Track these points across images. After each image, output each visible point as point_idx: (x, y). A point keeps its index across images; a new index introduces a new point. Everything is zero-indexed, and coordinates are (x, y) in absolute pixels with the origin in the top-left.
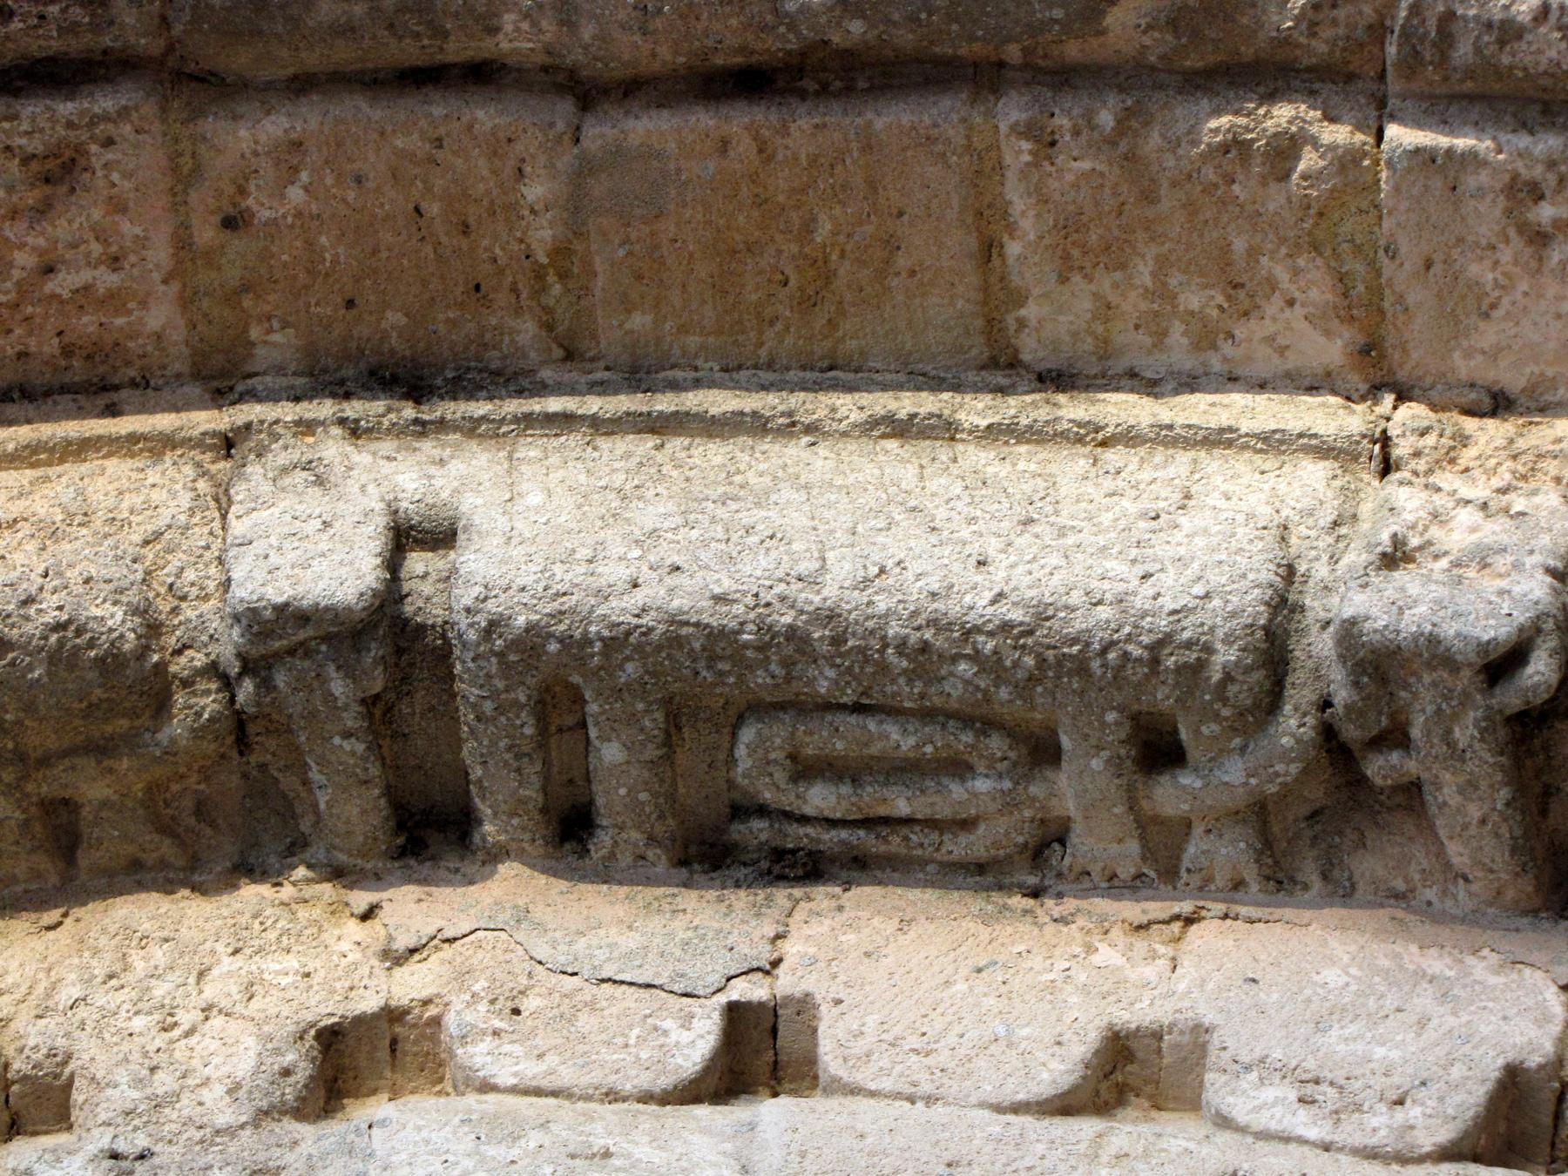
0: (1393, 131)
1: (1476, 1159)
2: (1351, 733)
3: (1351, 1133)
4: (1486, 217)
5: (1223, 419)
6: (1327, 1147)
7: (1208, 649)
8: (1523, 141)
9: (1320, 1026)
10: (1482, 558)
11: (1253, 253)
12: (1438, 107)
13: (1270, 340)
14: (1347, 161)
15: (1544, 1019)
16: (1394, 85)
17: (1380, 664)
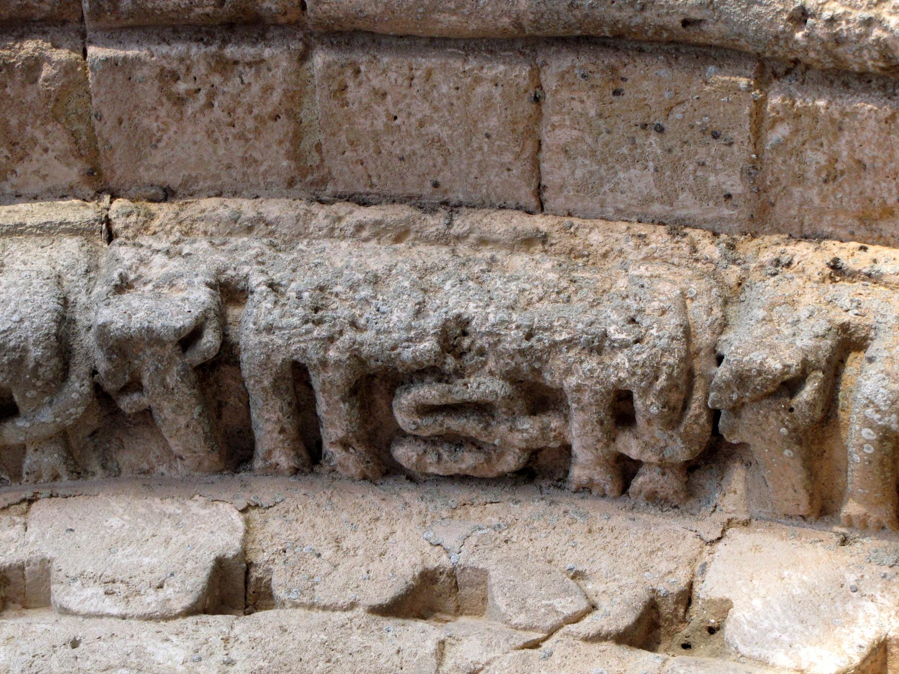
0: (91, 50)
1: (205, 612)
2: (109, 386)
3: (137, 607)
4: (149, 93)
5: (17, 219)
6: (124, 618)
7: (25, 350)
8: (164, 49)
9: (111, 551)
10: (170, 281)
11: (22, 125)
12: (117, 33)
13: (37, 172)
14: (68, 69)
15: (235, 529)
16: (89, 25)
17: (122, 347)
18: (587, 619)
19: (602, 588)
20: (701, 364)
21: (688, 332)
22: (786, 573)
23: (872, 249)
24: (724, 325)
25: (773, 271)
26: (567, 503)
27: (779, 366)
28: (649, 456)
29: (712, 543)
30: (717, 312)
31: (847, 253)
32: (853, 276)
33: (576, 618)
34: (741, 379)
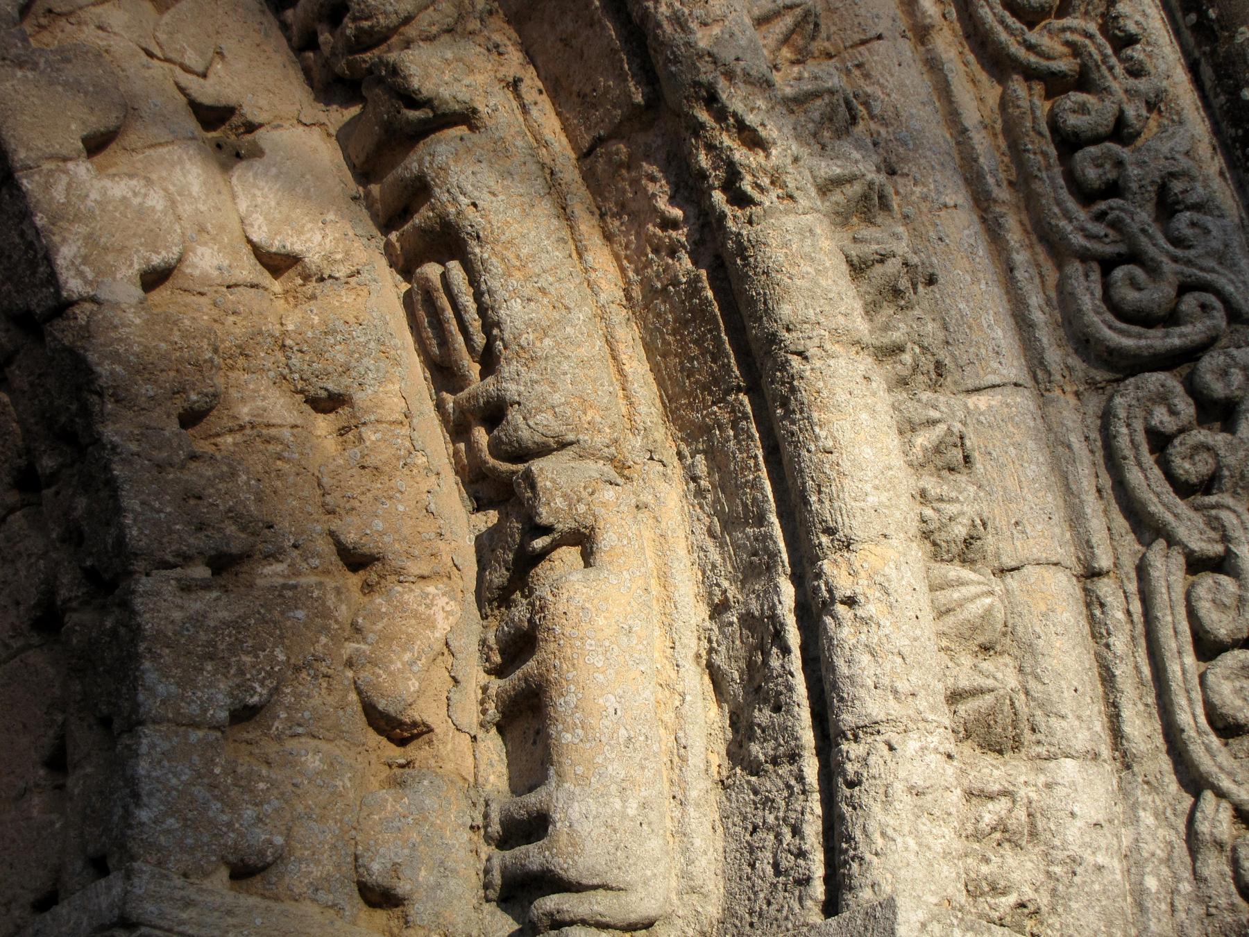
18: (190, 77)
19: (222, 74)
20: (394, 40)
21: (408, 20)
22: (308, 177)
23: (545, 96)
24: (430, 39)
25: (490, 47)
26: (270, 20)
27: (416, 86)
28: (326, 50)
29: (300, 121)
30: (434, 30)
31: (531, 83)
32: (518, 96)
33: (187, 69)
34: (394, 70)
